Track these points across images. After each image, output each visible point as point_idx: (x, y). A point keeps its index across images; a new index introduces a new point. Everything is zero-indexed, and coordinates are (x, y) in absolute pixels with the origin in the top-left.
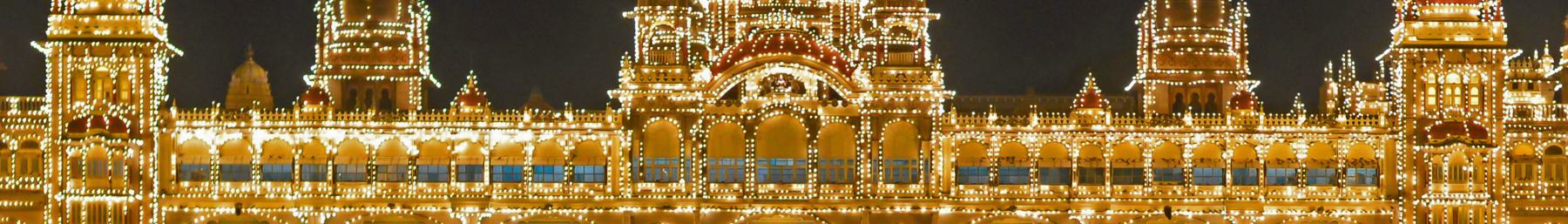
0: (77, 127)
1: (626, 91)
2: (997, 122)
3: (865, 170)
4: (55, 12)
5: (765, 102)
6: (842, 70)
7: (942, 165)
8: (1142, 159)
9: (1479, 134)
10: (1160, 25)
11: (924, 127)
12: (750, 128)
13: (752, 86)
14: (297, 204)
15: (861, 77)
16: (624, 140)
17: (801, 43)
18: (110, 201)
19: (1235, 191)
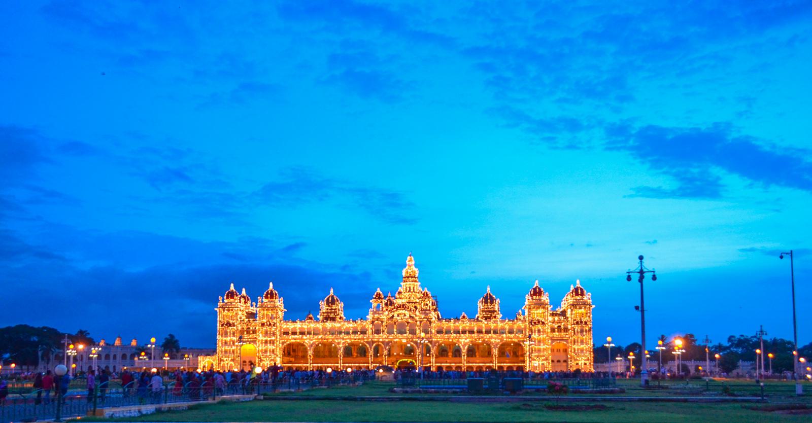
0: (263, 325)
1: (370, 317)
3: (418, 332)
5: (398, 318)
8: (474, 329)
12: (395, 323)
16: (371, 326)
19: (493, 335)
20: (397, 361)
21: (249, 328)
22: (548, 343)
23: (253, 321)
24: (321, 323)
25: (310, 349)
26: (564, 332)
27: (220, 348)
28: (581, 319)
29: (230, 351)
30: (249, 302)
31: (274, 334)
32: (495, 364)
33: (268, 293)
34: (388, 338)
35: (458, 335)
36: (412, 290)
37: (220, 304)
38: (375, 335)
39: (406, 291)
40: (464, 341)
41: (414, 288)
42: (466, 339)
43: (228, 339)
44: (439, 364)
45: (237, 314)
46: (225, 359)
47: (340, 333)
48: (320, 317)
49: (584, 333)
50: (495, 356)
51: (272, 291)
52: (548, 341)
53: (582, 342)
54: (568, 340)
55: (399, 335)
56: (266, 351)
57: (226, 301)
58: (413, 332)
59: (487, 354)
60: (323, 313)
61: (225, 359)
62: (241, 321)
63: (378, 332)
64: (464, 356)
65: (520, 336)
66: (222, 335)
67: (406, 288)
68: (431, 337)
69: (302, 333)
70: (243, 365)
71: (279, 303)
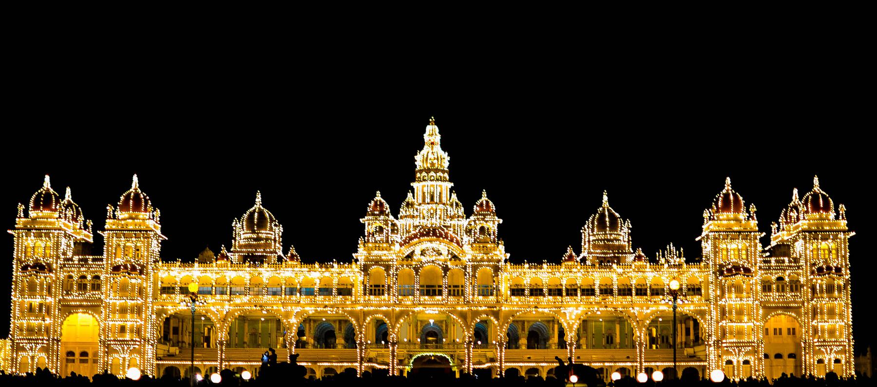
0: (116, 269)
1: (361, 254)
2: (530, 268)
3: (468, 290)
4: (110, 218)
5: (423, 259)
7: (504, 288)
8: (594, 285)
9: (747, 270)
10: (593, 231)
11: (497, 269)
13: (418, 252)
14: (214, 305)
15: (467, 248)
17: (440, 233)
18: (130, 303)
20: (411, 356)
21: (84, 277)
22: (757, 315)
23: (94, 260)
24: (248, 269)
25: (221, 328)
26: (792, 290)
27: (18, 321)
28: (826, 262)
29: (40, 330)
30: (81, 218)
31: (141, 292)
32: (641, 363)
33: (128, 198)
34: (400, 304)
36: (436, 199)
37: (20, 222)
38: (372, 297)
39: (424, 201)
40: (572, 313)
41: (440, 193)
42: (577, 307)
44: (534, 364)
45: (58, 245)
46: (28, 346)
47: (292, 291)
48: (235, 257)
49: (836, 293)
51: (137, 195)
52: (757, 310)
53: (831, 313)
54: (800, 307)
55: (426, 298)
56: (123, 329)
57: (33, 214)
59: (604, 341)
60: (240, 246)
61: (28, 346)
62: (65, 260)
63: (376, 290)
64: (571, 345)
66: (22, 292)
67: (424, 193)
68: (498, 302)
69: (625, 291)
70: (68, 361)
71: (149, 220)
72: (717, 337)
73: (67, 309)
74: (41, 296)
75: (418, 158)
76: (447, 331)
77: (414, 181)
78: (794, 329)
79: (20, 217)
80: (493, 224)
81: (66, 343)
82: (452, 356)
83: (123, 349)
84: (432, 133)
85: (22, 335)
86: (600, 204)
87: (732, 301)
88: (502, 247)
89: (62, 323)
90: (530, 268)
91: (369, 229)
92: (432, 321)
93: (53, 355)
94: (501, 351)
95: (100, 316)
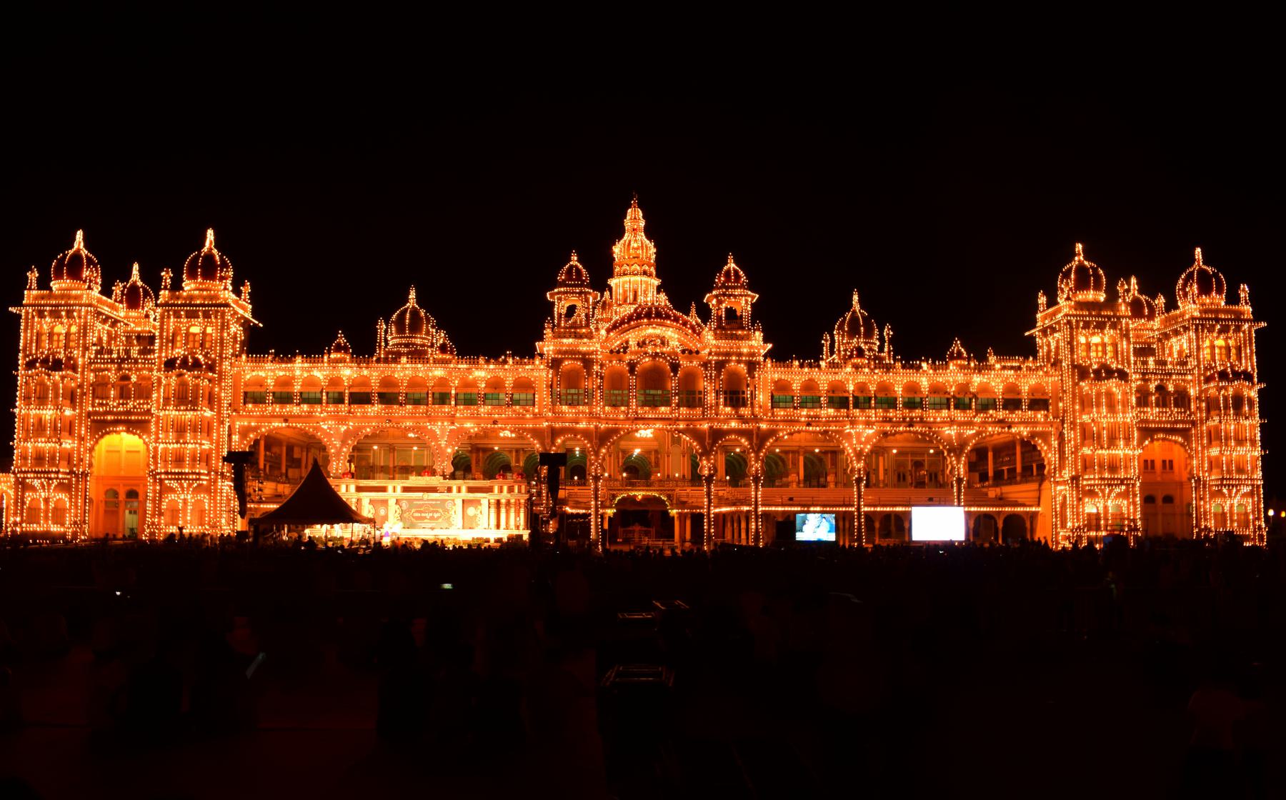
0: (170, 364)
1: (548, 346)
3: (711, 398)
6: (694, 331)
7: (762, 398)
11: (752, 366)
21: (127, 378)
27: (24, 446)
29: (53, 458)
31: (211, 400)
35: (844, 411)
37: (30, 295)
39: (625, 301)
40: (860, 434)
43: (48, 413)
46: (36, 483)
50: (959, 481)
53: (1240, 442)
54: (1189, 429)
58: (691, 398)
61: (36, 483)
64: (859, 480)
65: (1040, 416)
72: (1076, 470)
73: (101, 426)
74: (57, 406)
75: (617, 249)
76: (657, 464)
77: (612, 276)
78: (1171, 462)
79: (30, 289)
80: (744, 302)
81: (98, 478)
82: (669, 497)
83: (181, 485)
84: (634, 219)
85: (26, 465)
86: (849, 305)
87: (1101, 418)
88: (759, 335)
89: (92, 450)
90: (801, 366)
91: (561, 307)
92: (637, 451)
93: (77, 496)
94: (757, 488)
95: (149, 436)
